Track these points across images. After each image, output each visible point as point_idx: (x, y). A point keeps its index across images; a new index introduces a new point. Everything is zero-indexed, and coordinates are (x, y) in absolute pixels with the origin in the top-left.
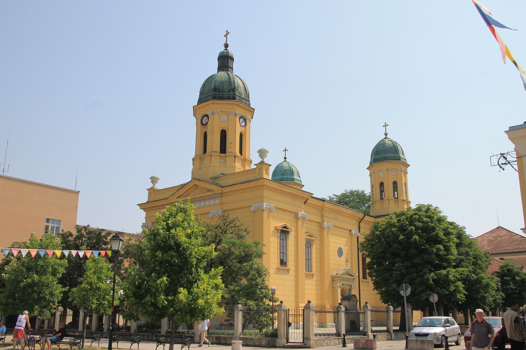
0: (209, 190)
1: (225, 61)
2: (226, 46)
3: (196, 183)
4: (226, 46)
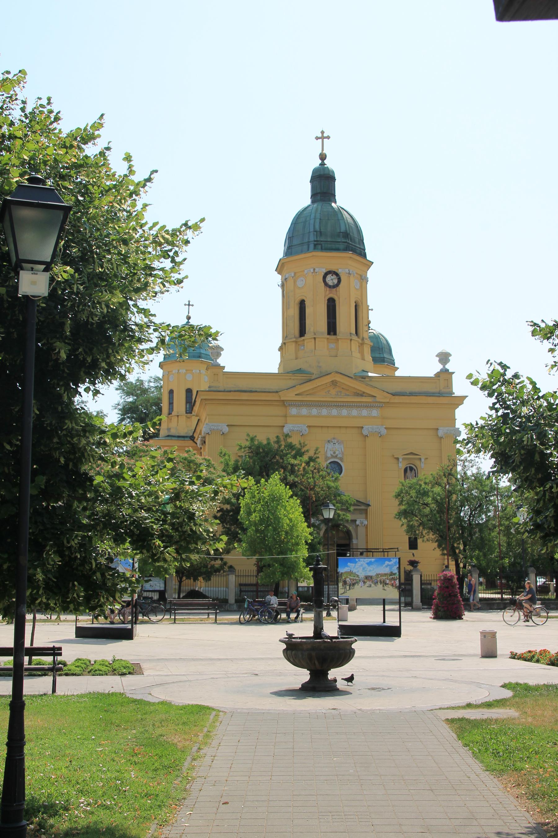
0: (362, 394)
2: (323, 157)
3: (338, 379)
4: (323, 157)
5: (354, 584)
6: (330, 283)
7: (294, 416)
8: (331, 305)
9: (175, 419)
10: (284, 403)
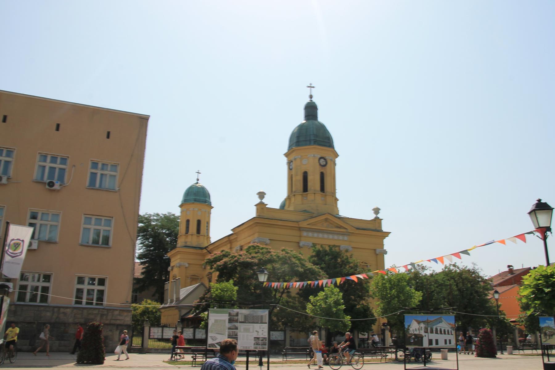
0: (340, 227)
1: (311, 110)
2: (311, 97)
4: (311, 97)
5: (552, 335)
6: (322, 164)
7: (305, 237)
8: (322, 176)
9: (190, 237)
10: (300, 229)
